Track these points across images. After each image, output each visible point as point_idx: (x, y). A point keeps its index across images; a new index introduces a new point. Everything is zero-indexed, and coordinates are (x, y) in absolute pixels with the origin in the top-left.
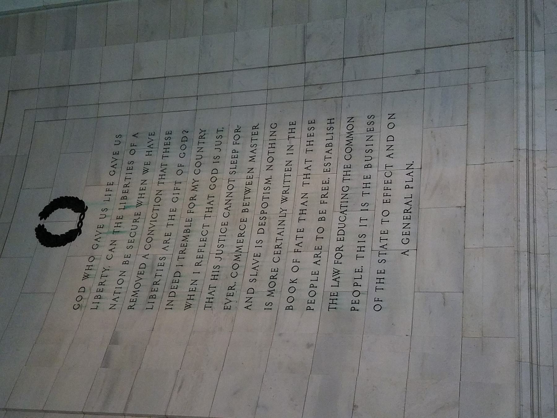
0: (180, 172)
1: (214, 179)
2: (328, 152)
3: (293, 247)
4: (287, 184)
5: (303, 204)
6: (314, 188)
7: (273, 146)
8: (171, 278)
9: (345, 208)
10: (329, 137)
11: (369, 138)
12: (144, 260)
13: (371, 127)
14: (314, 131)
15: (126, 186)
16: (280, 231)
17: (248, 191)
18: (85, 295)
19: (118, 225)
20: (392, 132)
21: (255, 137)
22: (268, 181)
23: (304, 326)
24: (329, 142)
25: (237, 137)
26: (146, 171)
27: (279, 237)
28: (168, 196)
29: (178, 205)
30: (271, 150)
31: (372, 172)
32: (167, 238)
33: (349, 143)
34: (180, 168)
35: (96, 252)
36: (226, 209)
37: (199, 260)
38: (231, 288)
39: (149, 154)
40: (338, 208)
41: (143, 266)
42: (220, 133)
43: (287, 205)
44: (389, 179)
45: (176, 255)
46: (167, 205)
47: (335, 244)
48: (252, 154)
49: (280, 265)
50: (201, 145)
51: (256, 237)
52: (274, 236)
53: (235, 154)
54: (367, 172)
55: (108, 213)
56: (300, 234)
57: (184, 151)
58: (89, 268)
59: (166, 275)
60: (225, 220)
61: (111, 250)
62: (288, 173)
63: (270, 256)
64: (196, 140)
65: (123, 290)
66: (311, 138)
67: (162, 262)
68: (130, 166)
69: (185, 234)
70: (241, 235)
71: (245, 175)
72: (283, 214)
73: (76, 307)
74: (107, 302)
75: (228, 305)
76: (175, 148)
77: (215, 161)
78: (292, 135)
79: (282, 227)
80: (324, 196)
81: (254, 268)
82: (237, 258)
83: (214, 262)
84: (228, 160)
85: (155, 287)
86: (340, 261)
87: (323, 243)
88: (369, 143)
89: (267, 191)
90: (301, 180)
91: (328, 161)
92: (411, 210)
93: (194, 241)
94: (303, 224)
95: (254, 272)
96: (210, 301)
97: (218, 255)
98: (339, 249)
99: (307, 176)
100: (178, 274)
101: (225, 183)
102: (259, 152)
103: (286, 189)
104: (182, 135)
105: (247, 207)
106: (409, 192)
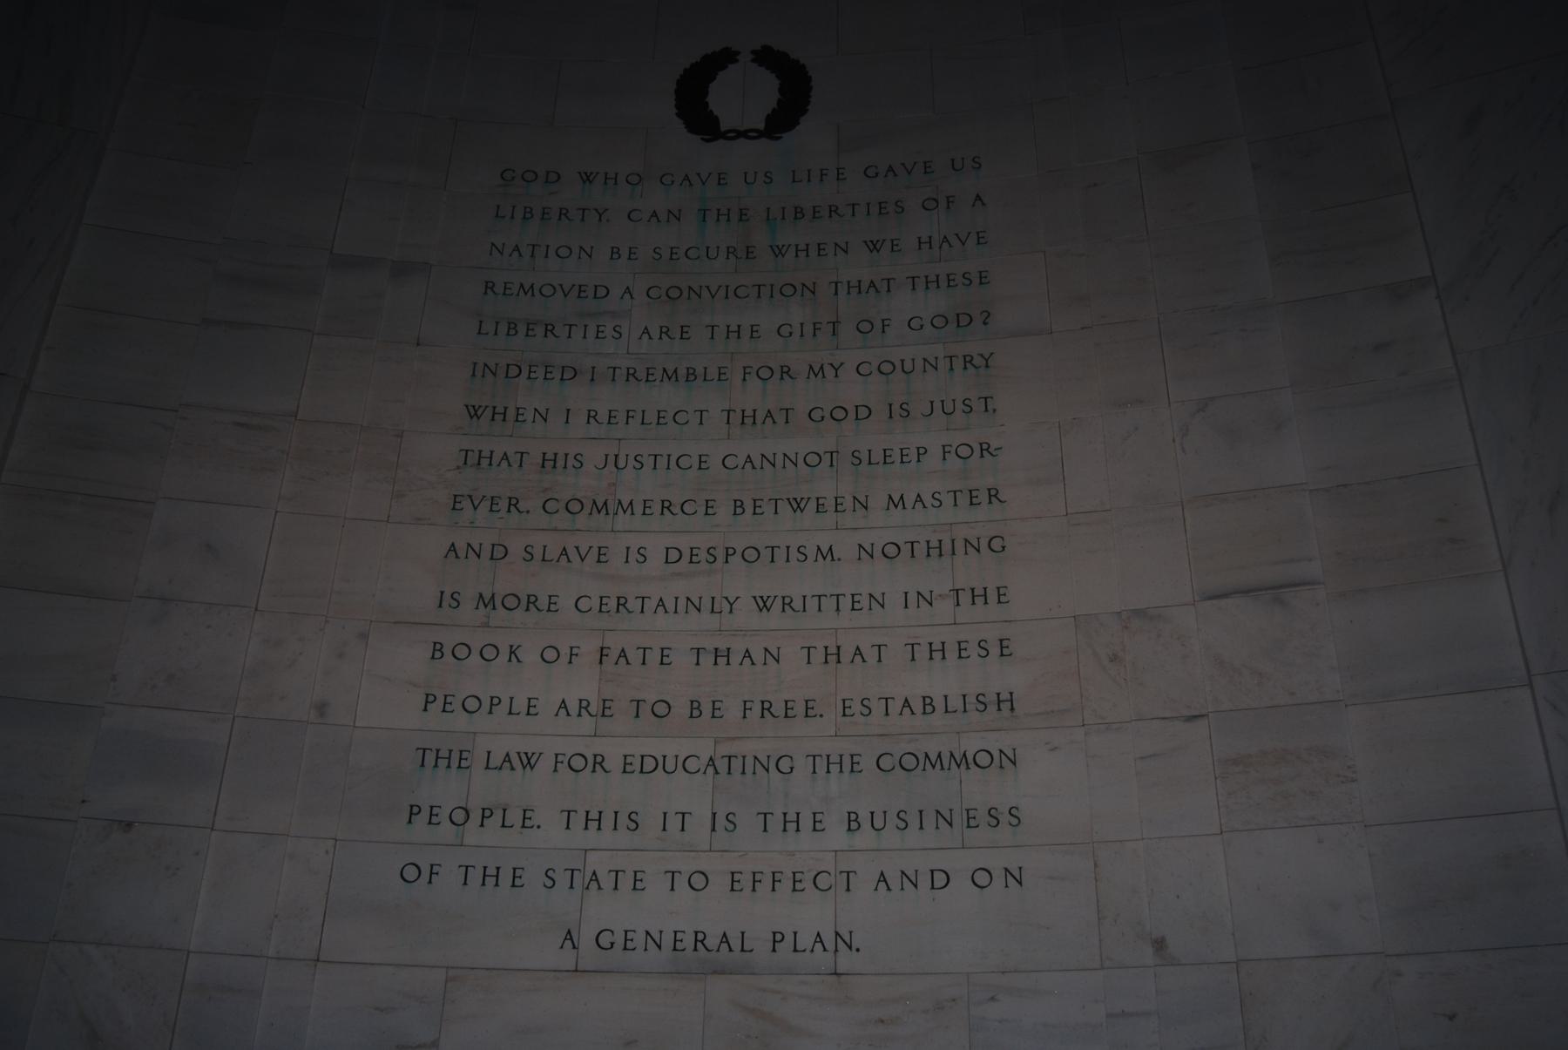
0: (865, 326)
1: (839, 414)
3: (614, 643)
4: (812, 604)
7: (934, 552)
10: (956, 703)
14: (974, 656)
16: (670, 605)
17: (797, 505)
21: (963, 500)
22: (827, 554)
25: (964, 451)
26: (874, 247)
27: (651, 604)
30: (920, 549)
31: (836, 836)
34: (878, 325)
38: (513, 503)
42: (979, 406)
48: (910, 499)
50: (943, 365)
56: (654, 657)
57: (928, 328)
61: (655, 214)
62: (846, 603)
66: (952, 653)
67: (608, 331)
69: (682, 372)
70: (666, 506)
75: (466, 503)
77: (896, 407)
78: (965, 598)
79: (682, 607)
80: (766, 708)
82: (601, 508)
85: (540, 330)
86: (563, 768)
91: (878, 707)
93: (667, 396)
95: (552, 553)
98: (599, 762)
99: (833, 656)
103: (797, 604)
105: (749, 510)
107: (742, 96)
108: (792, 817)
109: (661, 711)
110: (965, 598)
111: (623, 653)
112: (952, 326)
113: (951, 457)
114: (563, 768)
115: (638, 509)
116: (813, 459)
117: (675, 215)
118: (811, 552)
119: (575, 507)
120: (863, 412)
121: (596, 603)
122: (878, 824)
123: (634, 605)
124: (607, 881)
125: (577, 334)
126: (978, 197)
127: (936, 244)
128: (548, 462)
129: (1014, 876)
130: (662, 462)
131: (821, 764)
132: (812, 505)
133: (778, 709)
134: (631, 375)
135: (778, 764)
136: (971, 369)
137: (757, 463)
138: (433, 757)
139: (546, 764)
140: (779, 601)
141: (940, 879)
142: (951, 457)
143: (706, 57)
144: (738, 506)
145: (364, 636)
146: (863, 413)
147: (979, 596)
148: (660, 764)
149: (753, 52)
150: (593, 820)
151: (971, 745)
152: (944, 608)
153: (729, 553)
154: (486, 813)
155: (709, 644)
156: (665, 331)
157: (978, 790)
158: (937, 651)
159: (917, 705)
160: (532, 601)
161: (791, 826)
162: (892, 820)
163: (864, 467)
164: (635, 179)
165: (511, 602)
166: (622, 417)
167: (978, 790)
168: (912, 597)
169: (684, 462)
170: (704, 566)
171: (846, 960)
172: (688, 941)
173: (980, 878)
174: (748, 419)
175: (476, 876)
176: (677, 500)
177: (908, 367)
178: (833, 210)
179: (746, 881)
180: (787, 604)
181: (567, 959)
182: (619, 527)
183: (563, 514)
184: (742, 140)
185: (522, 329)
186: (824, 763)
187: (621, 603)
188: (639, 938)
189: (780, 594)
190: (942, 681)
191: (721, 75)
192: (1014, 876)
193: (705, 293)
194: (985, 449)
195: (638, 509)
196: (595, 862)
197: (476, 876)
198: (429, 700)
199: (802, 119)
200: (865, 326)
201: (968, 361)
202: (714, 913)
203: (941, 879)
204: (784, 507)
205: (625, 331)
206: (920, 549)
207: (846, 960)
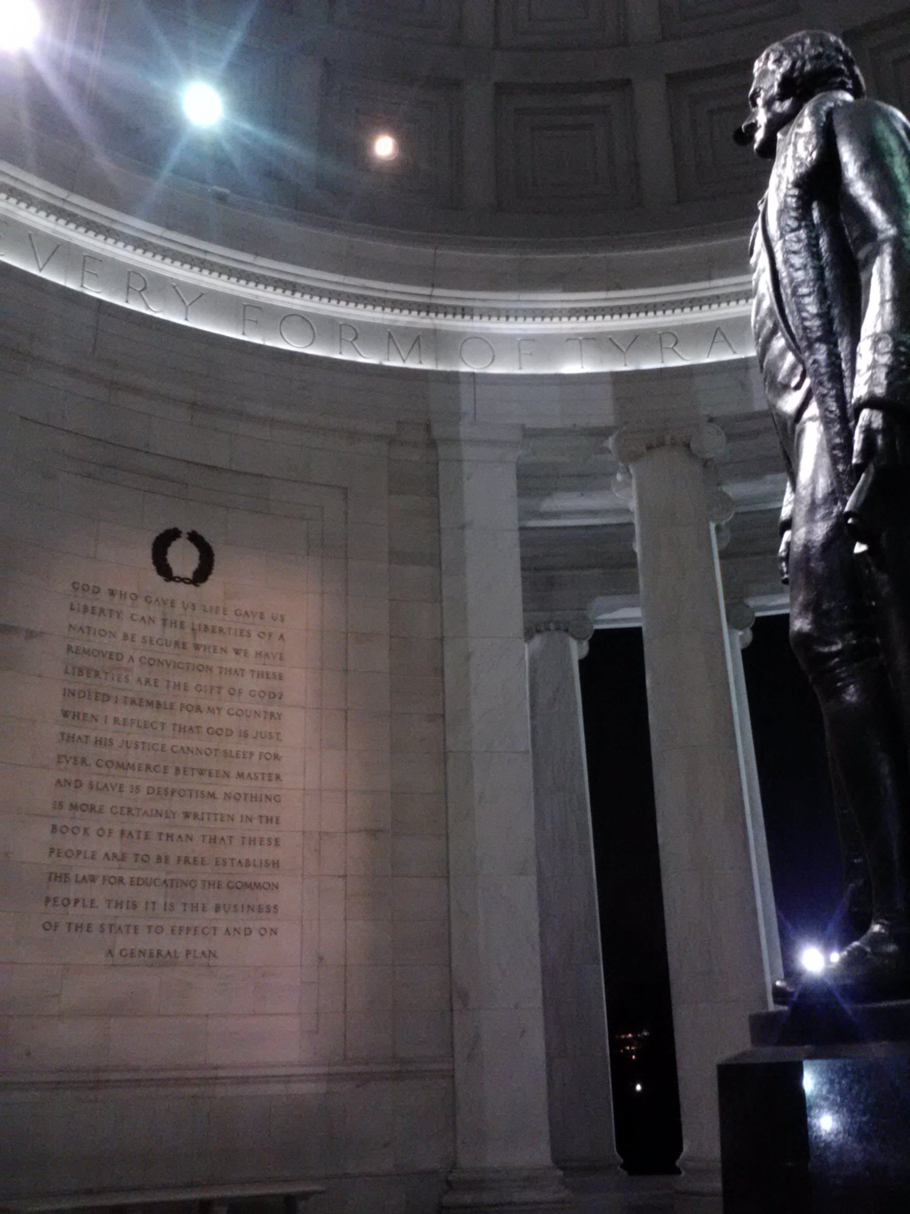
2: (240, 862)
3: (127, 827)
4: (206, 816)
5: (180, 837)
8: (102, 690)
10: (258, 863)
15: (221, 630)
19: (174, 624)
21: (266, 778)
22: (212, 795)
26: (237, 652)
30: (249, 797)
31: (211, 914)
32: (152, 683)
35: (141, 602)
36: (182, 748)
38: (84, 761)
39: (259, 654)
41: (120, 657)
42: (275, 736)
45: (131, 695)
47: (127, 875)
48: (246, 775)
50: (263, 715)
53: (248, 755)
55: (189, 610)
56: (142, 836)
58: (123, 595)
60: (168, 748)
61: (143, 618)
64: (270, 709)
67: (123, 678)
68: (245, 633)
69: (155, 703)
70: (148, 767)
72: (170, 815)
73: (76, 586)
74: (79, 619)
75: (63, 759)
76: (261, 684)
80: (187, 861)
81: (106, 786)
82: (121, 766)
85: (93, 674)
86: (107, 882)
88: (245, 909)
91: (229, 862)
93: (147, 714)
96: (70, 738)
98: (121, 880)
100: (106, 698)
101: (213, 746)
103: (200, 817)
106: (182, 956)
107: (183, 558)
109: (145, 859)
112: (267, 697)
113: (263, 759)
114: (107, 882)
121: (119, 810)
124: (124, 929)
126: (282, 636)
128: (98, 742)
129: (274, 932)
131: (207, 884)
132: (207, 773)
133: (191, 860)
134: (133, 702)
135: (190, 884)
138: (54, 877)
144: (177, 770)
146: (229, 733)
147: (269, 820)
149: (188, 533)
150: (119, 905)
151: (261, 880)
155: (166, 831)
157: (265, 898)
158: (252, 841)
160: (92, 808)
167: (265, 898)
169: (155, 747)
172: (155, 953)
173: (263, 932)
175: (73, 927)
176: (152, 764)
179: (177, 930)
180: (196, 816)
184: (181, 585)
187: (129, 810)
188: (137, 953)
192: (274, 932)
194: (276, 757)
197: (73, 927)
198: (52, 851)
199: (211, 577)
201: (272, 715)
202: (165, 942)
204: (196, 773)
206: (249, 797)
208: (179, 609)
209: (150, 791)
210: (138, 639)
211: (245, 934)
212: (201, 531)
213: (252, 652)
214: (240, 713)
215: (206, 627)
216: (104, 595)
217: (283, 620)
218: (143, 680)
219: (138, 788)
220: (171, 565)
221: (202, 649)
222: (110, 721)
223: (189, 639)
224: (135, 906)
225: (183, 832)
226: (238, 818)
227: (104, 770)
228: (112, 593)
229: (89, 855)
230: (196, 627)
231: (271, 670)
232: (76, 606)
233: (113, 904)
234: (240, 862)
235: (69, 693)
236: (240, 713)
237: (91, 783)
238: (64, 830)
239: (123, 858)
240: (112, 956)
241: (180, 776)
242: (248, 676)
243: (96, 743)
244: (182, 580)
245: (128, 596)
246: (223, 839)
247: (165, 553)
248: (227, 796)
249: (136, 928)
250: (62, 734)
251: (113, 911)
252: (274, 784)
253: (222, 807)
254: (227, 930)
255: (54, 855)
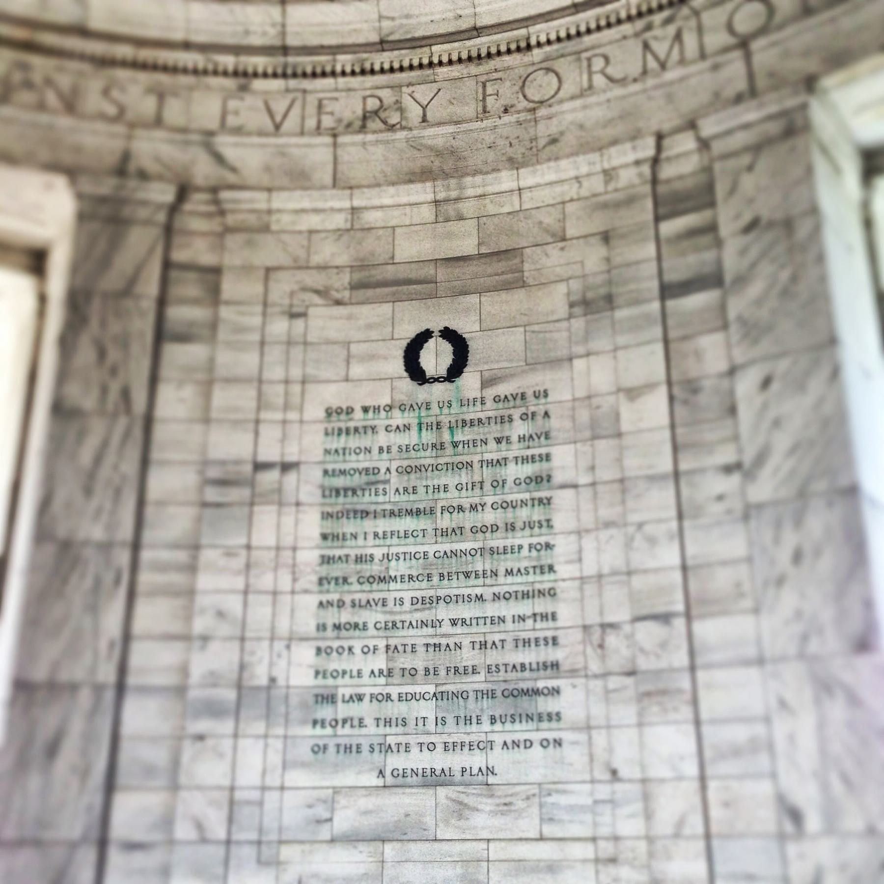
0: (495, 484)
1: (484, 529)
2: (514, 667)
3: (392, 642)
4: (474, 622)
6: (468, 657)
8: (359, 507)
9: (440, 698)
11: (529, 717)
12: (383, 471)
13: (545, 717)
16: (414, 624)
17: (467, 575)
18: (343, 417)
19: (429, 427)
20: (536, 745)
21: (538, 571)
22: (480, 598)
23: (299, 670)
24: (527, 666)
26: (499, 441)
28: (464, 477)
29: (453, 493)
30: (520, 595)
31: (486, 726)
33: (526, 693)
34: (501, 483)
35: (396, 413)
37: (381, 535)
38: (345, 580)
39: (521, 439)
40: (441, 689)
42: (545, 524)
43: (446, 628)
44: (475, 747)
45: (388, 507)
46: (450, 479)
47: (394, 691)
48: (515, 571)
49: (372, 631)
50: (530, 503)
51: (407, 596)
52: (407, 617)
53: (516, 550)
54: (485, 719)
55: (446, 411)
56: (409, 649)
57: (523, 484)
58: (377, 409)
59: (365, 500)
60: (431, 555)
62: (488, 621)
63: (381, 618)
64: (537, 495)
65: (347, 457)
67: (381, 491)
70: (411, 577)
71: (488, 567)
72: (436, 624)
75: (325, 582)
76: (528, 470)
78: (538, 618)
79: (419, 626)
80: (456, 670)
81: (368, 602)
82: (382, 580)
83: (378, 553)
84: (509, 542)
85: (350, 493)
87: (396, 679)
89: (466, 598)
90: (479, 639)
91: (502, 668)
92: (434, 779)
93: (408, 523)
94: (421, 650)
95: (363, 603)
97: (387, 557)
98: (388, 697)
99: (483, 645)
100: (365, 514)
101: (477, 545)
102: (519, 579)
103: (468, 622)
104: (544, 476)
105: (446, 578)
106: (458, 774)
107: (436, 357)
108: (468, 718)
109: (413, 673)
110: (538, 618)
111: (396, 647)
112: (533, 483)
113: (533, 550)
115: (399, 580)
116: (473, 552)
117: (407, 427)
118: (473, 597)
119: (371, 580)
120: (495, 528)
121: (383, 625)
122: (503, 720)
123: (399, 625)
124: (395, 748)
125: (367, 493)
127: (527, 439)
128: (359, 559)
129: (558, 743)
130: (408, 556)
132: (473, 574)
133: (461, 670)
135: (463, 695)
136: (542, 506)
137: (449, 554)
139: (367, 699)
140: (460, 622)
141: (528, 744)
142: (533, 550)
143: (418, 335)
144: (441, 575)
145: (288, 647)
146: (495, 528)
147: (544, 617)
148: (413, 696)
150: (388, 722)
151: (541, 684)
152: (530, 623)
153: (438, 599)
154: (345, 721)
155: (432, 641)
156: (406, 490)
157: (545, 705)
158: (526, 643)
159: (519, 668)
160: (356, 626)
161: (468, 722)
162: (509, 718)
163: (495, 556)
164: (387, 408)
165: (348, 626)
166: (389, 535)
167: (545, 705)
168: (516, 618)
169: (417, 556)
170: (428, 605)
171: (491, 780)
172: (429, 771)
173: (545, 744)
174: (444, 533)
175: (342, 749)
176: (415, 574)
177: (514, 504)
178: (480, 421)
179: (451, 746)
180: (464, 622)
181: (380, 782)
182: (391, 588)
183: (367, 584)
185: (342, 493)
186: (481, 694)
187: (394, 624)
189: (461, 617)
190: (528, 656)
191: (426, 345)
192: (558, 743)
193: (423, 469)
194: (548, 546)
195: (399, 580)
196: (391, 740)
197: (342, 749)
198: (317, 673)
200: (495, 484)
201: (540, 501)
202: (439, 760)
203: (528, 744)
204: (461, 576)
205: (388, 491)
206: (520, 595)
207: (491, 780)
208: (435, 410)
209: (414, 601)
210: (395, 449)
211: (525, 747)
212: (453, 326)
213: (514, 438)
214: (506, 505)
215: (464, 422)
216: (358, 414)
217: (546, 395)
218: (401, 491)
219: (401, 600)
220: (424, 368)
221: (461, 446)
222: (370, 537)
223: (446, 437)
224: (405, 724)
225: (451, 641)
226: (509, 619)
227: (366, 587)
228: (365, 410)
229: (355, 673)
230: (454, 424)
231: (536, 451)
232: (330, 430)
233: (382, 723)
234: (514, 667)
235: (326, 516)
236: (506, 505)
237: (353, 602)
238: (328, 651)
239: (390, 673)
240: (384, 777)
241: (446, 582)
242: (511, 466)
243: (356, 561)
244: (436, 380)
245: (382, 408)
246: (494, 643)
247: (418, 357)
248: (496, 597)
249: (407, 746)
250: (323, 557)
251: (382, 730)
252: (547, 577)
253: (492, 609)
254: (505, 743)
255: (320, 676)
